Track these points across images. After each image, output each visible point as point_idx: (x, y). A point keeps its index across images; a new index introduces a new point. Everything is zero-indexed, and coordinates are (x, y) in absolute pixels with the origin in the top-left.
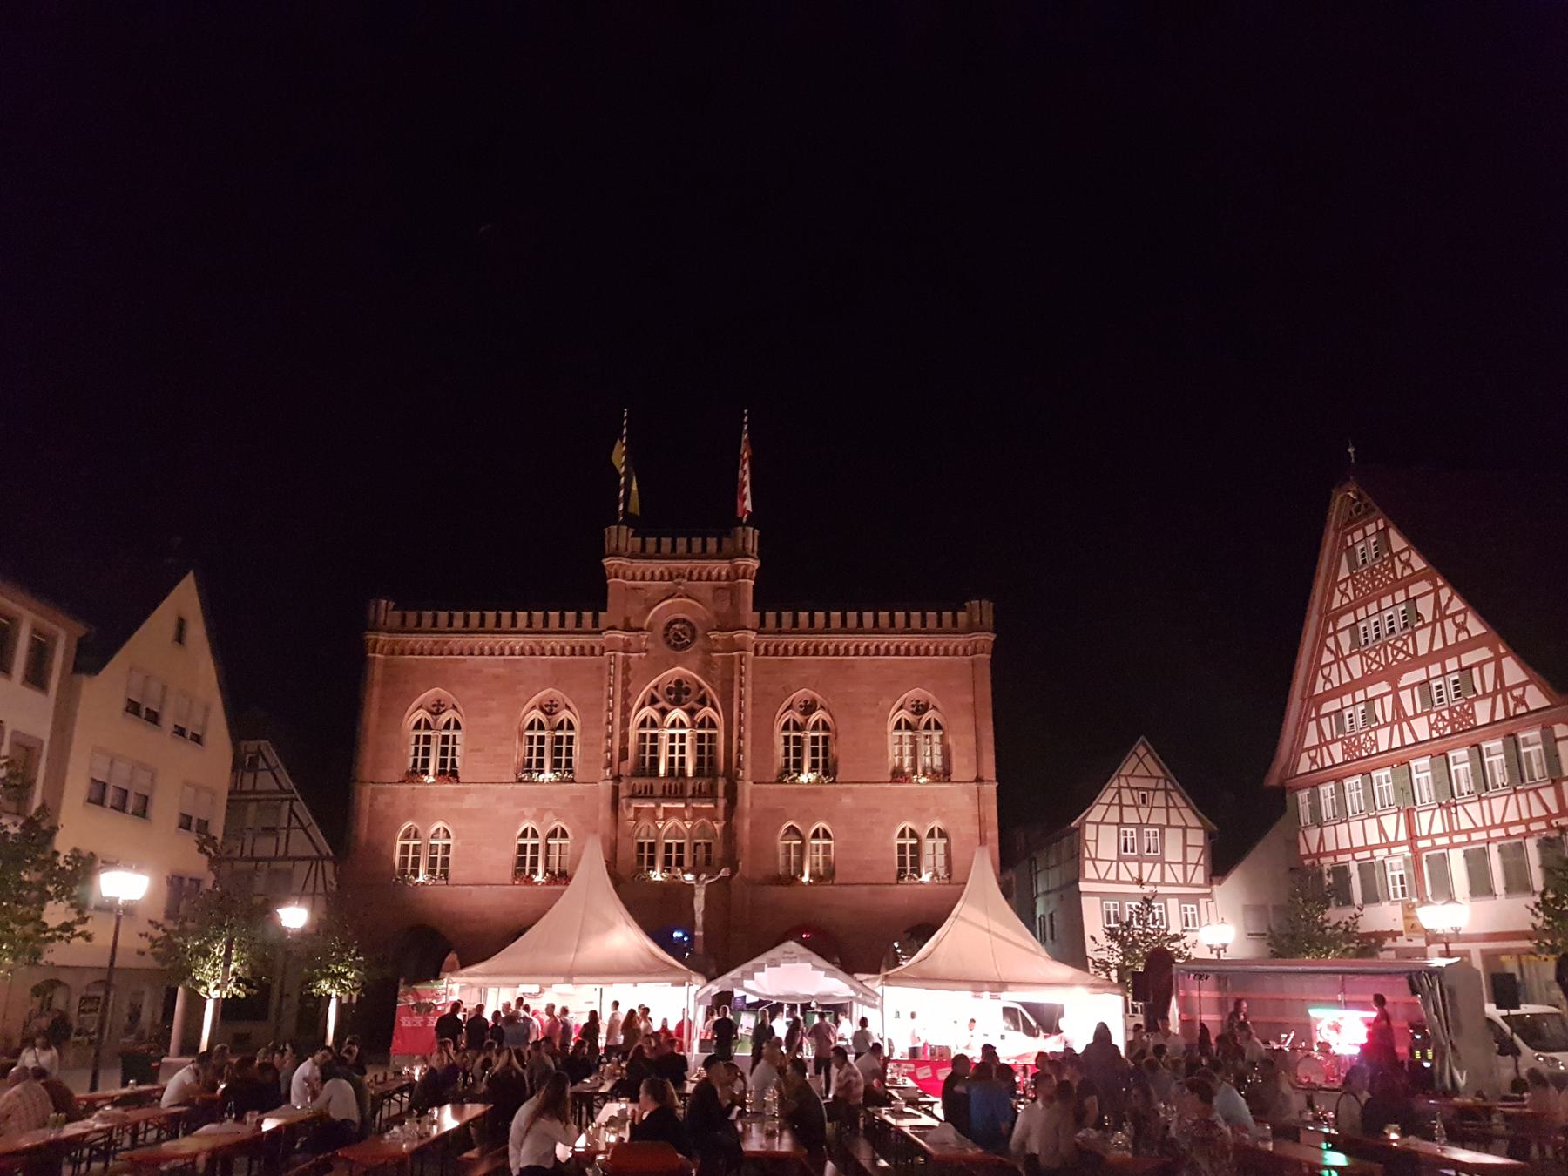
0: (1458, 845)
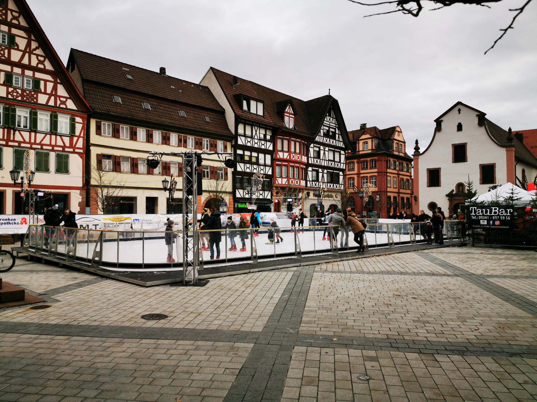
0: (34, 149)
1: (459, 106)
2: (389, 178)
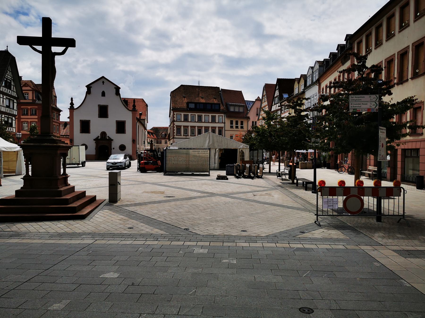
1: (103, 80)
2: (54, 126)
